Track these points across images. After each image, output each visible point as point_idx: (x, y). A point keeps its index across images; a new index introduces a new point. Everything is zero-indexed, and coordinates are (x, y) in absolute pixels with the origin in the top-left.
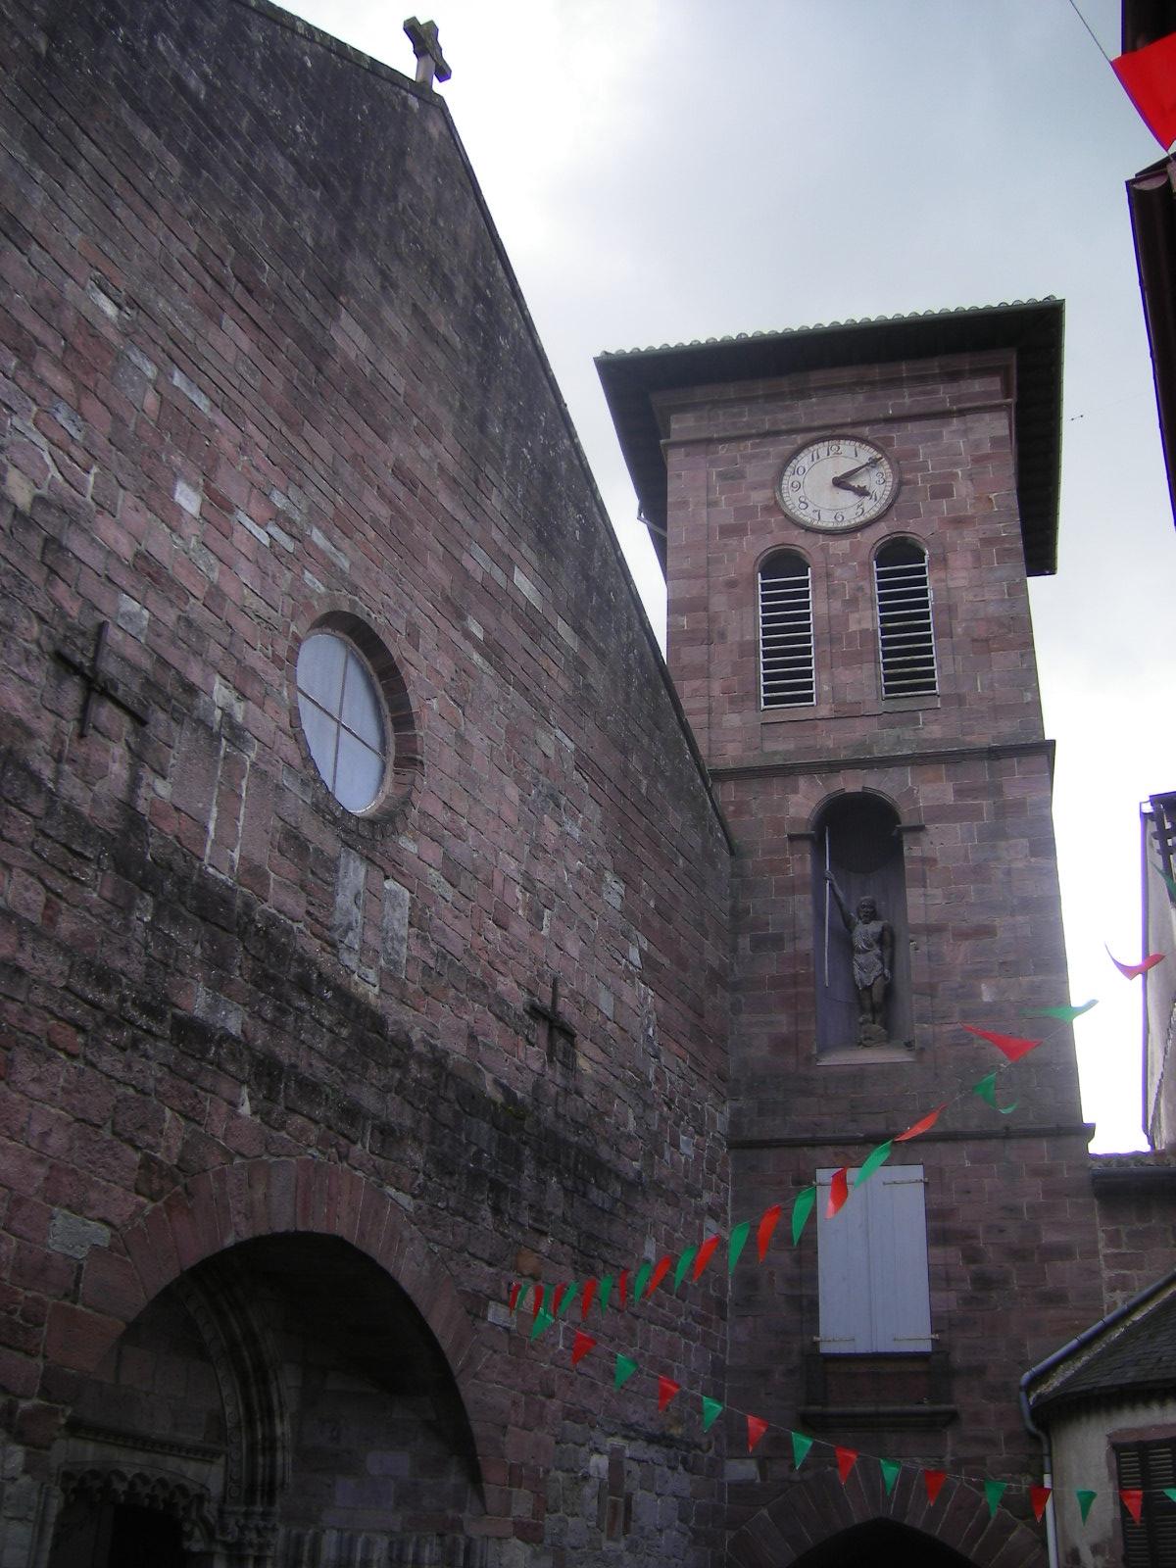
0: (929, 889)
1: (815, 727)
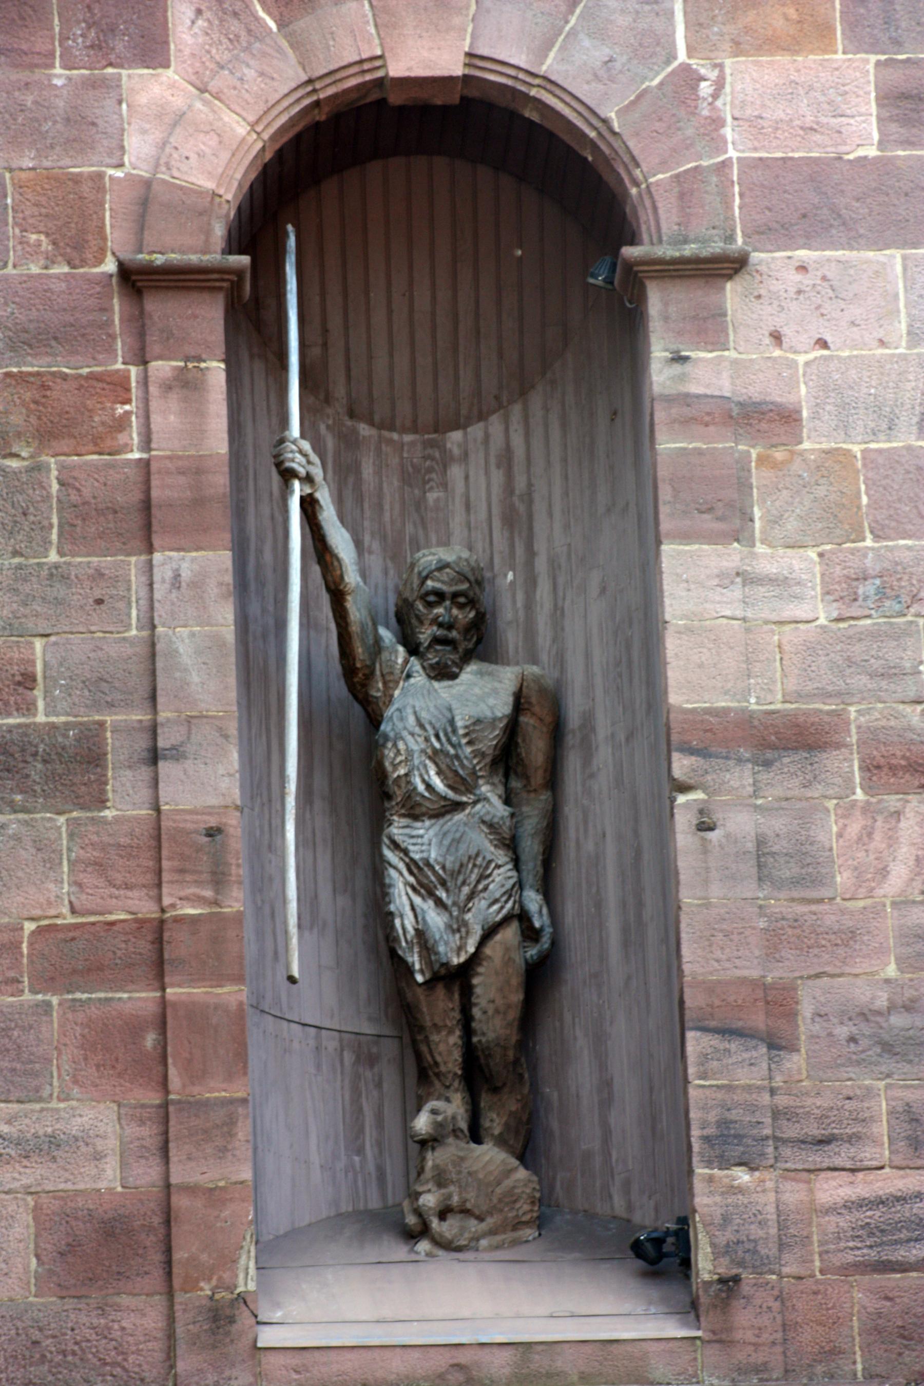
0: (760, 548)
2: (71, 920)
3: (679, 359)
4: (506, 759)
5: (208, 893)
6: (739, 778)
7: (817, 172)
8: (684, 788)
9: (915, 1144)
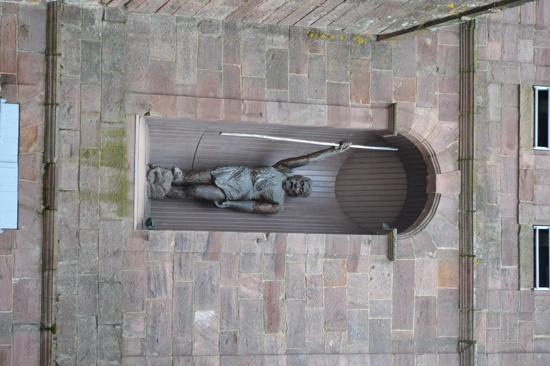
0: (324, 260)
1: (510, 146)
2: (241, 77)
3: (369, 242)
4: (262, 200)
5: (246, 112)
6: (269, 250)
7: (411, 280)
8: (267, 236)
9: (179, 289)
